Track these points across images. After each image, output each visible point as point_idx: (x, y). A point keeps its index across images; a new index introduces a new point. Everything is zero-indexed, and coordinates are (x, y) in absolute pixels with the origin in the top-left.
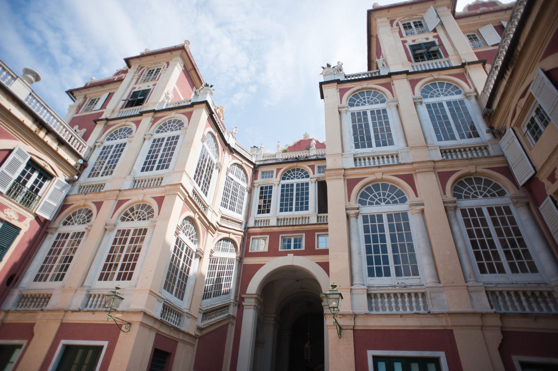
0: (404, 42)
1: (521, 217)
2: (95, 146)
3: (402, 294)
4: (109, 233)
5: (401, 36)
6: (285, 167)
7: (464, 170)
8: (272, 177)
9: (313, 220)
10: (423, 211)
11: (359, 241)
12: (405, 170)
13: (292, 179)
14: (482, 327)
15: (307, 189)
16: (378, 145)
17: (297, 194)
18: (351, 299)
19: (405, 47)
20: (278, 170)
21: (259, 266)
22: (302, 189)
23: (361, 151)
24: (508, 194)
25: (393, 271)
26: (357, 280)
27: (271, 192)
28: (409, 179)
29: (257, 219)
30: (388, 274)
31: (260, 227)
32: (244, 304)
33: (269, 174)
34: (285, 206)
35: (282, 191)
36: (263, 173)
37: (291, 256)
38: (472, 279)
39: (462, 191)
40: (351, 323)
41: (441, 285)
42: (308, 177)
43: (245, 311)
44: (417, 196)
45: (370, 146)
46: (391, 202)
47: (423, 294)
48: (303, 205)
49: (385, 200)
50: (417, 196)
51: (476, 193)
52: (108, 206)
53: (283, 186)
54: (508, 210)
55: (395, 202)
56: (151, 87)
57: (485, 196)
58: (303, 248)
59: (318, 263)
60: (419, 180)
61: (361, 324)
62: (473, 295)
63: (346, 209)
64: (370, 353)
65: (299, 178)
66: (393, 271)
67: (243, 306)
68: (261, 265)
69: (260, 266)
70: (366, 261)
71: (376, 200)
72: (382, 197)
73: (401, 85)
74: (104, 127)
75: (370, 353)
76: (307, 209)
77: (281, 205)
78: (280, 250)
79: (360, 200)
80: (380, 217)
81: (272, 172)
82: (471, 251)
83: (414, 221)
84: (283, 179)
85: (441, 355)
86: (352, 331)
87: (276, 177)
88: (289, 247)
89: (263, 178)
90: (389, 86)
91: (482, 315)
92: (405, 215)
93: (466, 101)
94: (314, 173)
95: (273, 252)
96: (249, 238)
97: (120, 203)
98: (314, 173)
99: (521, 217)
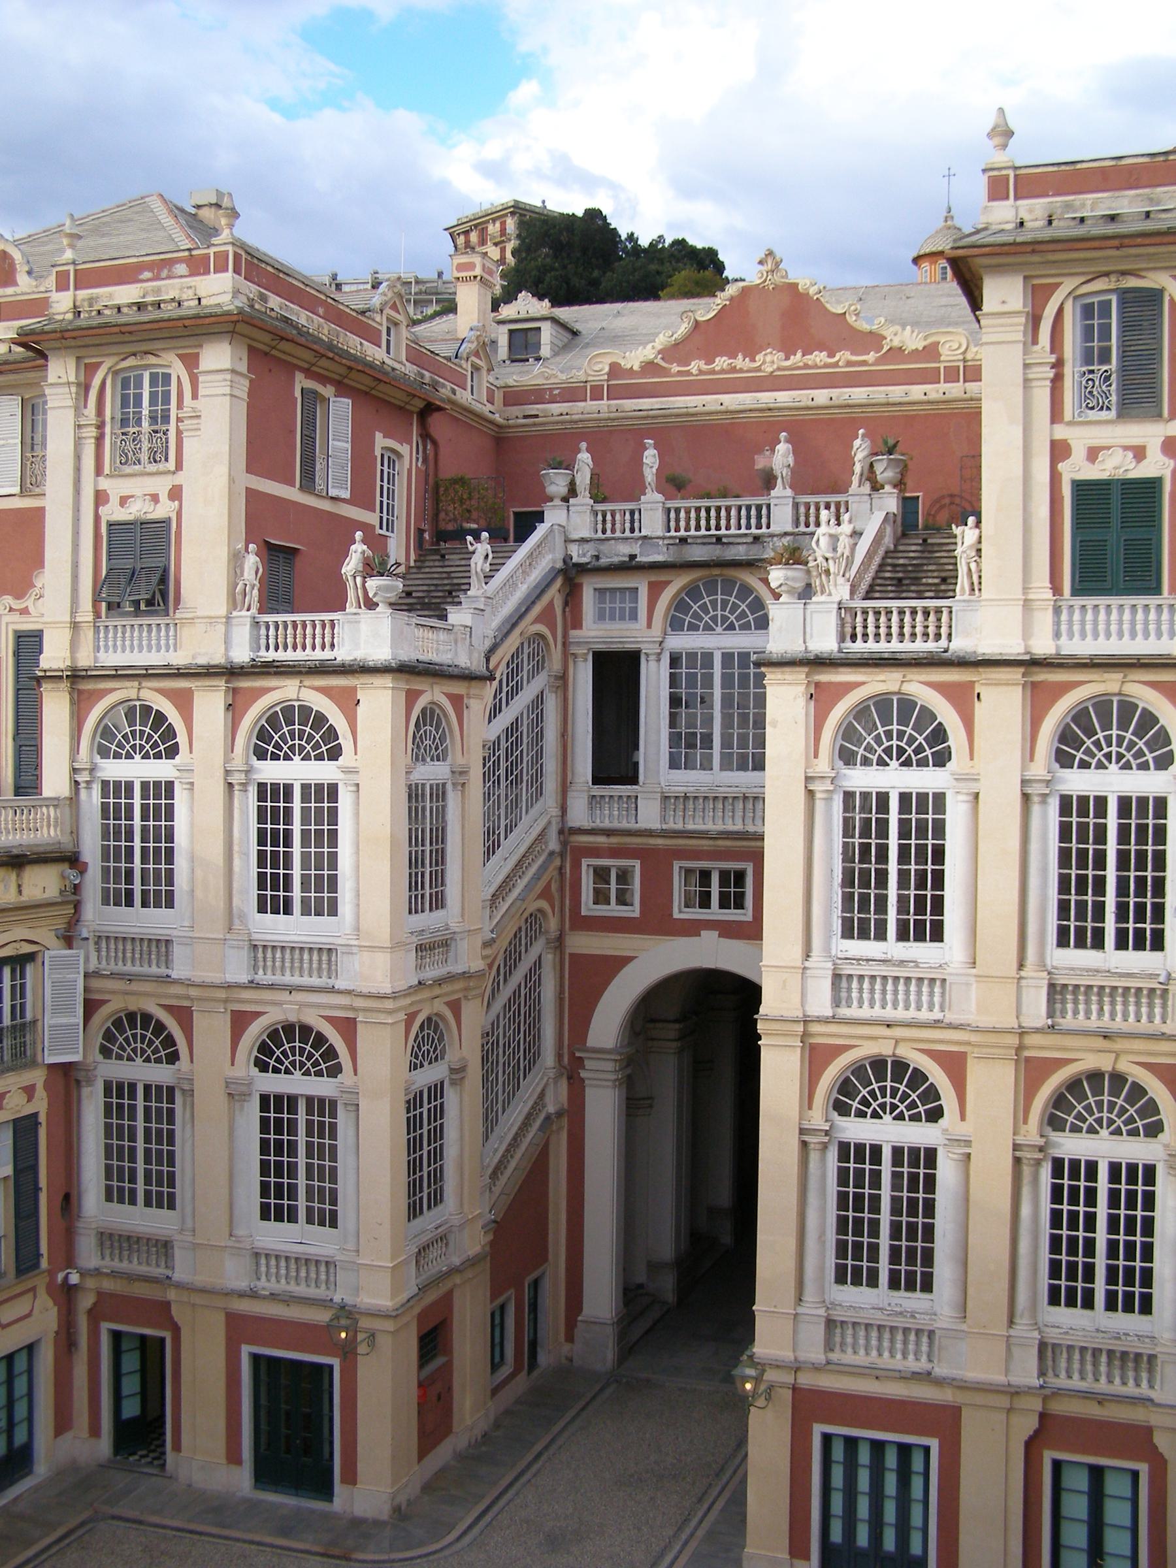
0: (1059, 451)
2: (77, 783)
3: (893, 1329)
4: (242, 1108)
5: (1056, 415)
6: (678, 583)
7: (1090, 1062)
8: (634, 616)
10: (969, 1155)
11: (823, 1209)
12: (947, 1040)
13: (708, 628)
14: (1009, 1410)
16: (903, 936)
17: (727, 701)
18: (795, 1332)
19: (1055, 478)
20: (655, 590)
21: (615, 964)
22: (744, 679)
23: (857, 947)
25: (884, 1277)
26: (809, 1295)
28: (955, 1065)
30: (873, 1282)
31: (608, 833)
32: (583, 1074)
33: (618, 606)
34: (687, 747)
38: (1024, 1321)
39: (1070, 1108)
40: (789, 1379)
41: (964, 1327)
43: (589, 1092)
44: (963, 1117)
45: (881, 936)
46: (906, 1114)
47: (931, 1334)
49: (894, 1107)
50: (963, 1117)
51: (1099, 1121)
52: (212, 1029)
54: (1150, 1171)
55: (915, 1118)
56: (164, 509)
57: (1118, 1132)
60: (975, 1073)
61: (806, 1380)
62: (1015, 1350)
63: (802, 1131)
64: (818, 1429)
65: (731, 627)
66: (884, 1277)
67: (583, 1080)
68: (627, 960)
69: (623, 962)
70: (834, 1252)
71: (874, 1105)
72: (888, 1100)
73: (1001, 703)
74: (72, 702)
75: (818, 1429)
78: (679, 912)
79: (837, 1100)
80: (876, 1150)
82: (1045, 1256)
83: (946, 1172)
84: (676, 625)
85: (934, 1444)
86: (790, 1392)
87: (649, 626)
88: (705, 902)
89: (601, 616)
90: (964, 699)
91: (1014, 1392)
92: (931, 1155)
95: (657, 922)
96: (576, 866)
97: (240, 1021)
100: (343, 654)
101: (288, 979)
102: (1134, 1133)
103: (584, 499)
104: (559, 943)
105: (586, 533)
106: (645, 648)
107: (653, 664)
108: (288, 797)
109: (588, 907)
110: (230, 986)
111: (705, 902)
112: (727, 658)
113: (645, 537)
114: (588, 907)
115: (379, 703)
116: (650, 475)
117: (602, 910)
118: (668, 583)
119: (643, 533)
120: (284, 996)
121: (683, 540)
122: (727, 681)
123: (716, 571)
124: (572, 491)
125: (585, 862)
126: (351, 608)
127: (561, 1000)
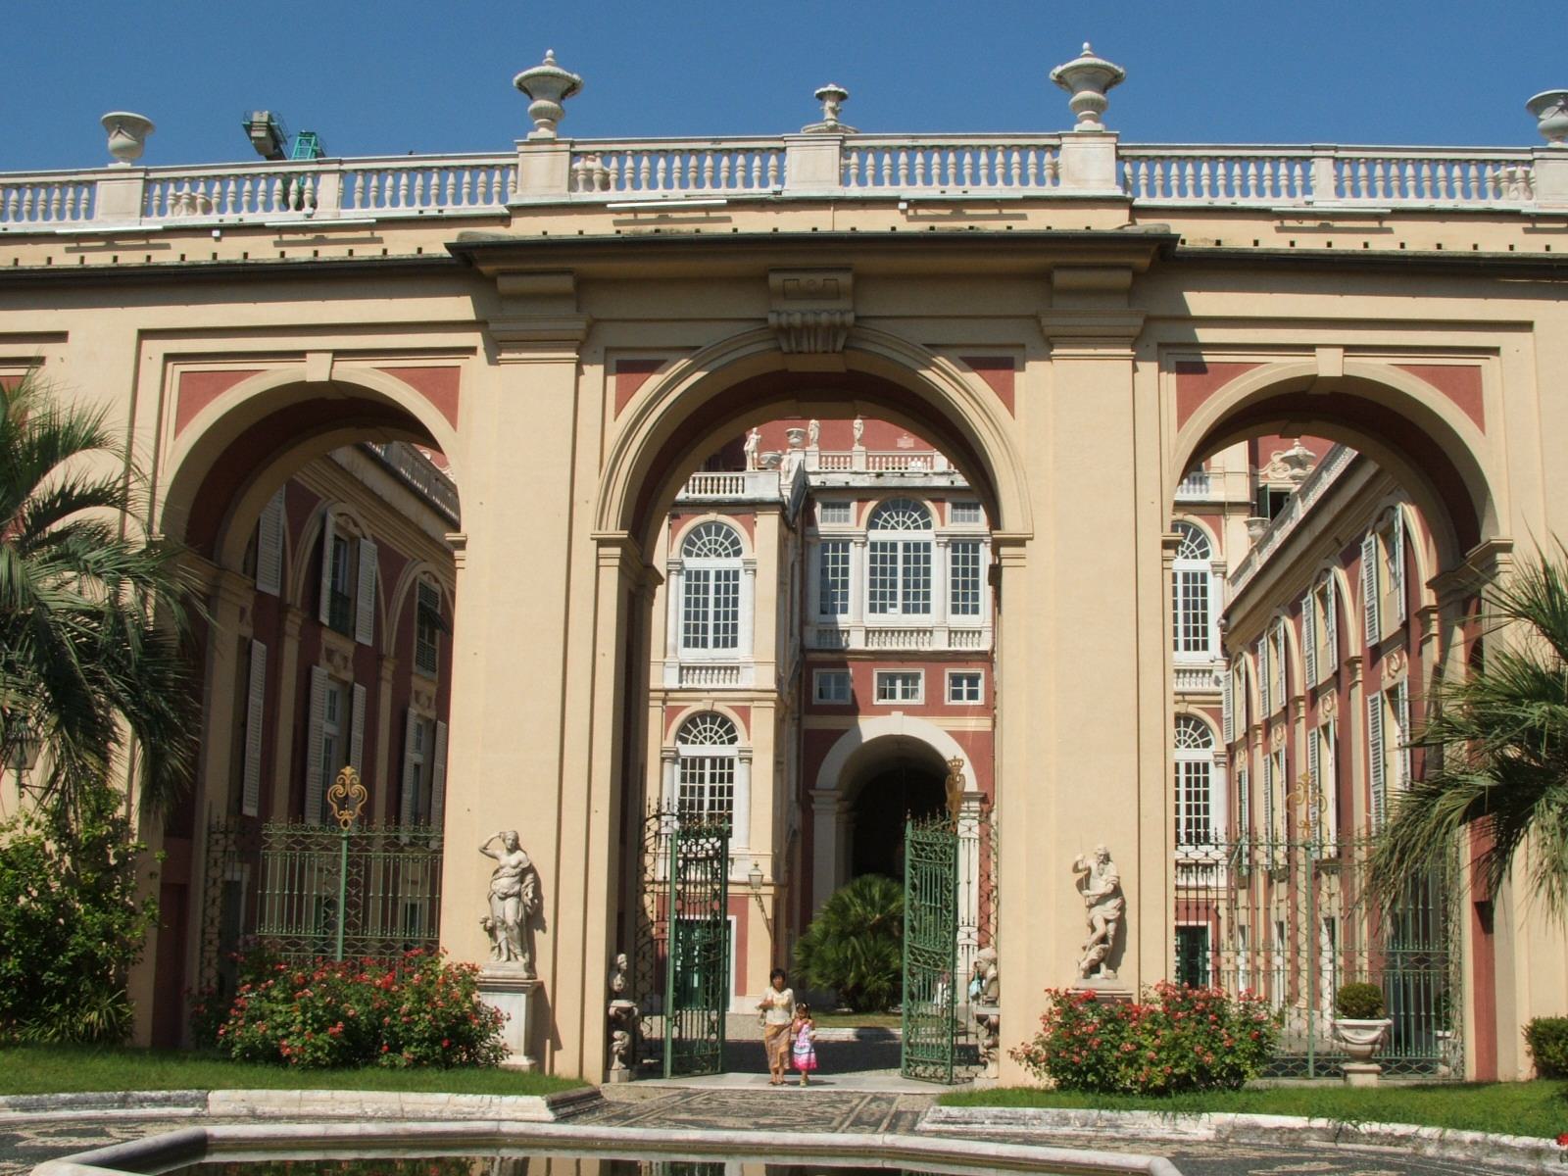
1: (1217, 777)
8: (846, 519)
9: (940, 643)
13: (893, 528)
15: (927, 560)
24: (1212, 748)
27: (846, 560)
29: (822, 628)
34: (879, 602)
35: (873, 559)
36: (825, 506)
37: (897, 715)
42: (928, 526)
43: (816, 818)
48: (918, 602)
53: (873, 546)
54: (1206, 766)
58: (919, 699)
59: (950, 733)
65: (908, 528)
76: (927, 609)
77: (873, 596)
81: (847, 506)
84: (872, 525)
88: (893, 696)
93: (1210, 576)
94: (943, 524)
98: (943, 524)
99: (1217, 777)
100: (749, 494)
101: (703, 685)
102: (1197, 746)
103: (814, 447)
104: (799, 726)
105: (817, 469)
106: (855, 539)
107: (859, 549)
108: (707, 578)
109: (816, 700)
110: (667, 691)
111: (893, 696)
112: (907, 547)
113: (856, 473)
114: (816, 700)
115: (768, 525)
116: (857, 434)
117: (824, 702)
118: (867, 500)
119: (854, 469)
120: (705, 695)
121: (879, 475)
122: (906, 560)
123: (901, 493)
124: (805, 441)
125: (815, 671)
126: (749, 467)
127: (798, 757)
